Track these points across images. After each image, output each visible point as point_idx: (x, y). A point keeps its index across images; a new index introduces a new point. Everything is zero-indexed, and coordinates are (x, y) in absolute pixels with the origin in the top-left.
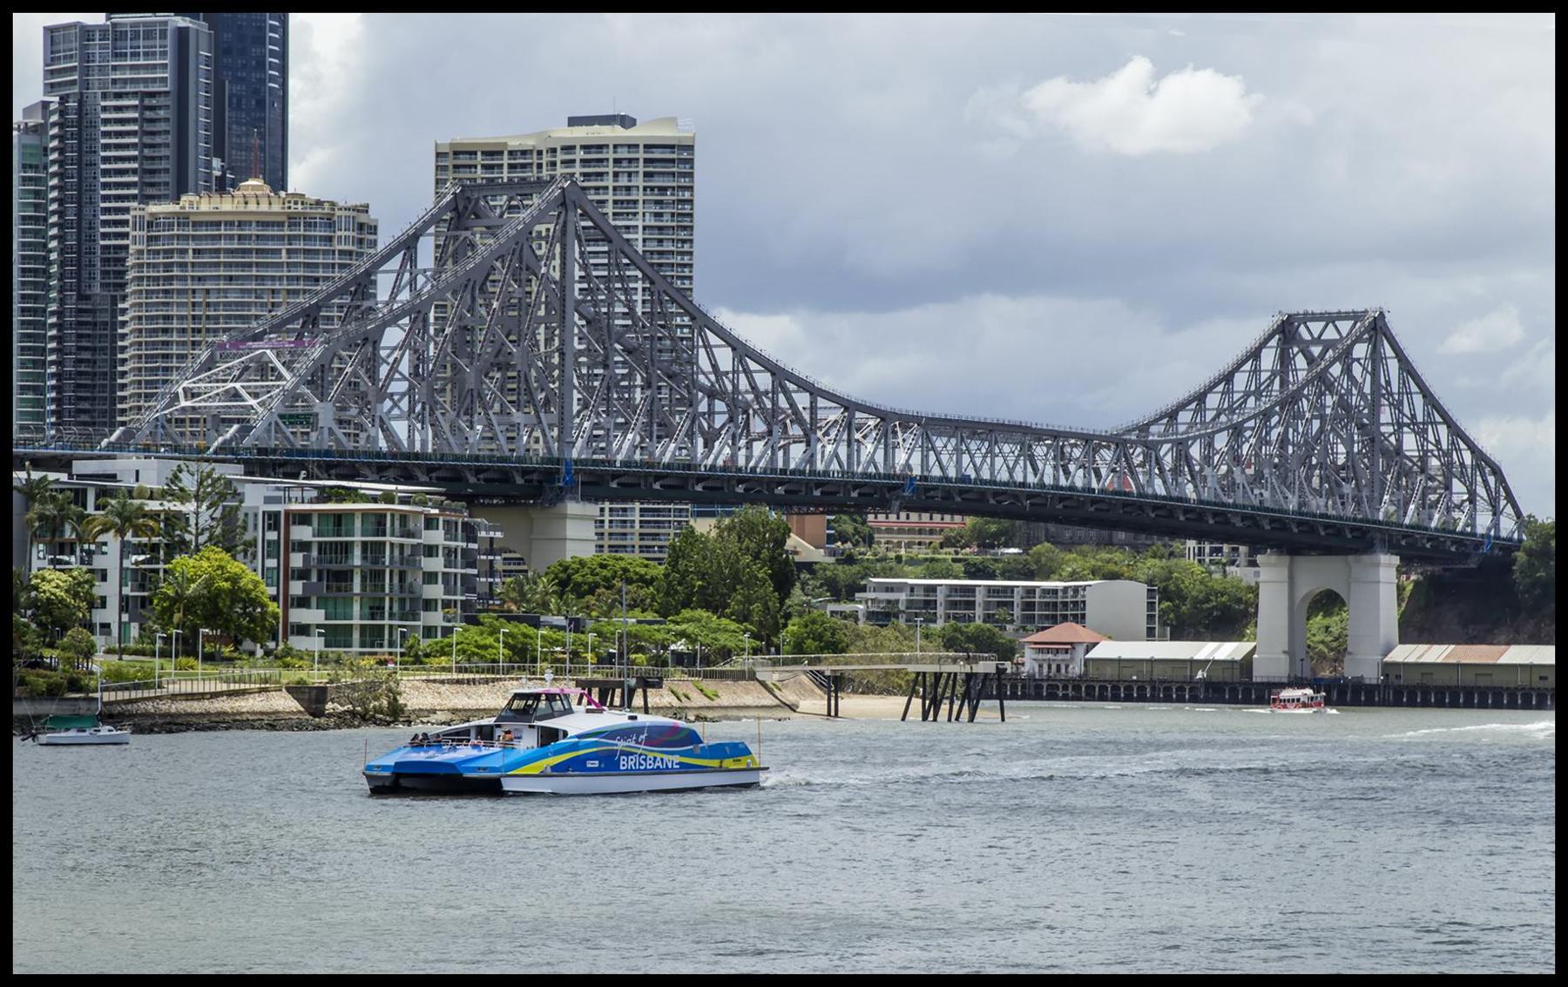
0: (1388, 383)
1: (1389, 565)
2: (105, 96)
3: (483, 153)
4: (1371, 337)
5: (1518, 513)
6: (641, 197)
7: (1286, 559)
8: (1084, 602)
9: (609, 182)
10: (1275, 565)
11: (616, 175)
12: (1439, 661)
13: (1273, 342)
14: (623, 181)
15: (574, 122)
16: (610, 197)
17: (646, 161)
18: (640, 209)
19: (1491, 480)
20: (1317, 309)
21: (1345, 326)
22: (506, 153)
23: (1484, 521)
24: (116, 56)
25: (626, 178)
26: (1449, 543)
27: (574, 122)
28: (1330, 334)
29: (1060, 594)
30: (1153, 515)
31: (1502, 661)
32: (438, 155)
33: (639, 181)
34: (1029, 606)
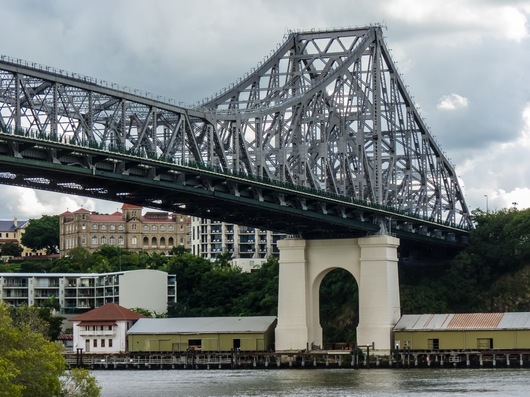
0: (385, 90)
1: (392, 246)
4: (372, 49)
5: (465, 210)
7: (302, 243)
8: (117, 288)
10: (293, 248)
12: (445, 327)
13: (288, 54)
19: (449, 179)
20: (323, 27)
21: (348, 42)
23: (445, 215)
26: (425, 230)
28: (335, 48)
29: (96, 282)
30: (213, 189)
31: (500, 326)
34: (71, 292)
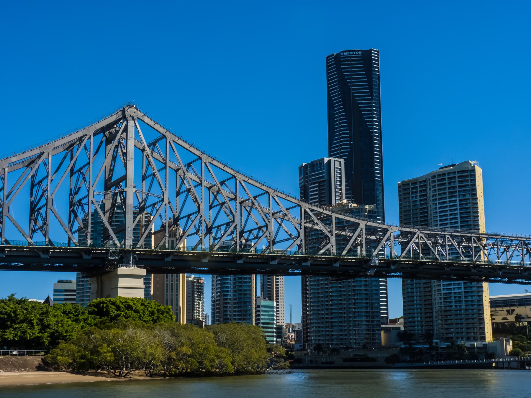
2: (311, 184)
3: (412, 184)
6: (457, 190)
9: (447, 186)
11: (449, 183)
14: (453, 185)
15: (440, 168)
16: (447, 191)
17: (459, 177)
18: (457, 194)
22: (418, 182)
24: (314, 171)
25: (453, 184)
27: (440, 168)
32: (399, 187)
33: (457, 184)
